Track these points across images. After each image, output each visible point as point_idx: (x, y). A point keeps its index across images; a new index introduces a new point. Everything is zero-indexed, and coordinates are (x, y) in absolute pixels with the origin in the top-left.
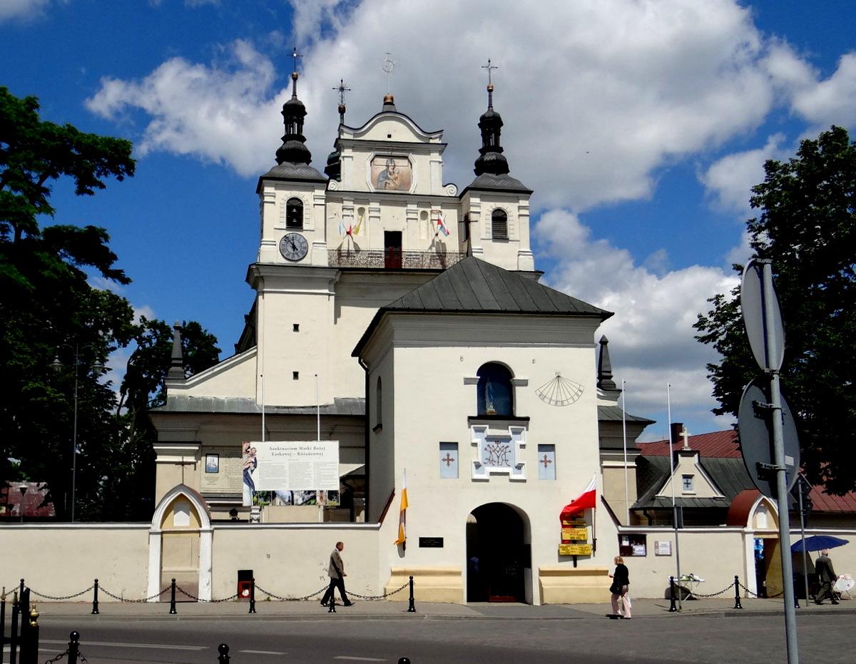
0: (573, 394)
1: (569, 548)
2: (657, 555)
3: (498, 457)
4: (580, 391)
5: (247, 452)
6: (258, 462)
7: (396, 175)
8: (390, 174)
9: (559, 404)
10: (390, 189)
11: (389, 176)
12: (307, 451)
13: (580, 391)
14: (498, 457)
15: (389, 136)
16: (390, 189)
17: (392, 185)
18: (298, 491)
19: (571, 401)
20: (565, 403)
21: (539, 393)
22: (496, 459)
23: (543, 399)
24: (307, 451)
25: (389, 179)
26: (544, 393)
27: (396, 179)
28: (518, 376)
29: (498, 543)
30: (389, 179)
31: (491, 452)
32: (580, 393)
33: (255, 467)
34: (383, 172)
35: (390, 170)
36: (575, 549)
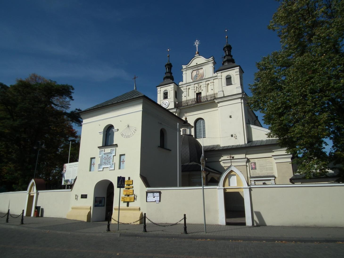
0: (133, 132)
1: (125, 198)
2: (160, 201)
3: (107, 161)
4: (136, 130)
5: (65, 167)
6: (66, 170)
7: (199, 75)
8: (198, 75)
9: (128, 137)
10: (198, 79)
11: (197, 76)
12: (76, 166)
13: (136, 130)
14: (107, 161)
15: (197, 64)
16: (198, 79)
17: (198, 78)
18: (73, 179)
19: (132, 135)
20: (130, 136)
21: (121, 134)
22: (106, 162)
23: (122, 136)
24: (76, 166)
25: (197, 77)
26: (123, 134)
27: (199, 76)
28: (116, 128)
29: (105, 195)
30: (197, 77)
31: (105, 160)
32: (135, 131)
33: (66, 172)
34: (196, 75)
35: (198, 74)
36: (128, 199)
